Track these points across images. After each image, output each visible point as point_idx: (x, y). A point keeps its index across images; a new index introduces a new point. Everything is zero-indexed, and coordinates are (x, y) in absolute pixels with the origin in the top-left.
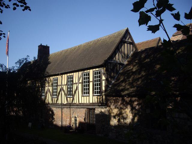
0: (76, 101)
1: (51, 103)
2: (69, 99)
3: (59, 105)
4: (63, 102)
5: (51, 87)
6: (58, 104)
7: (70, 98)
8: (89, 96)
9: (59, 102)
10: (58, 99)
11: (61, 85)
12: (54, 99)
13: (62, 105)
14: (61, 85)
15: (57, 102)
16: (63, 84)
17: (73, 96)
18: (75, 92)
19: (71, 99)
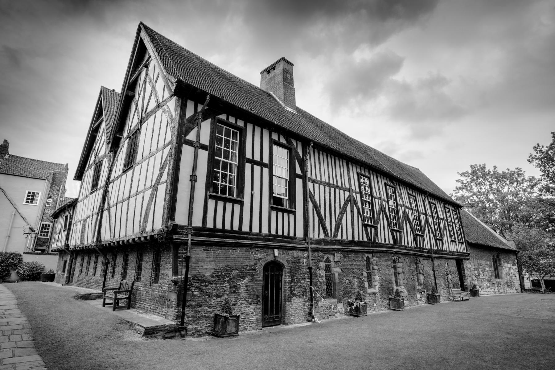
0: (446, 248)
2: (438, 241)
3: (428, 253)
9: (427, 246)
10: (424, 240)
11: (425, 214)
12: (418, 237)
13: (431, 251)
15: (423, 245)
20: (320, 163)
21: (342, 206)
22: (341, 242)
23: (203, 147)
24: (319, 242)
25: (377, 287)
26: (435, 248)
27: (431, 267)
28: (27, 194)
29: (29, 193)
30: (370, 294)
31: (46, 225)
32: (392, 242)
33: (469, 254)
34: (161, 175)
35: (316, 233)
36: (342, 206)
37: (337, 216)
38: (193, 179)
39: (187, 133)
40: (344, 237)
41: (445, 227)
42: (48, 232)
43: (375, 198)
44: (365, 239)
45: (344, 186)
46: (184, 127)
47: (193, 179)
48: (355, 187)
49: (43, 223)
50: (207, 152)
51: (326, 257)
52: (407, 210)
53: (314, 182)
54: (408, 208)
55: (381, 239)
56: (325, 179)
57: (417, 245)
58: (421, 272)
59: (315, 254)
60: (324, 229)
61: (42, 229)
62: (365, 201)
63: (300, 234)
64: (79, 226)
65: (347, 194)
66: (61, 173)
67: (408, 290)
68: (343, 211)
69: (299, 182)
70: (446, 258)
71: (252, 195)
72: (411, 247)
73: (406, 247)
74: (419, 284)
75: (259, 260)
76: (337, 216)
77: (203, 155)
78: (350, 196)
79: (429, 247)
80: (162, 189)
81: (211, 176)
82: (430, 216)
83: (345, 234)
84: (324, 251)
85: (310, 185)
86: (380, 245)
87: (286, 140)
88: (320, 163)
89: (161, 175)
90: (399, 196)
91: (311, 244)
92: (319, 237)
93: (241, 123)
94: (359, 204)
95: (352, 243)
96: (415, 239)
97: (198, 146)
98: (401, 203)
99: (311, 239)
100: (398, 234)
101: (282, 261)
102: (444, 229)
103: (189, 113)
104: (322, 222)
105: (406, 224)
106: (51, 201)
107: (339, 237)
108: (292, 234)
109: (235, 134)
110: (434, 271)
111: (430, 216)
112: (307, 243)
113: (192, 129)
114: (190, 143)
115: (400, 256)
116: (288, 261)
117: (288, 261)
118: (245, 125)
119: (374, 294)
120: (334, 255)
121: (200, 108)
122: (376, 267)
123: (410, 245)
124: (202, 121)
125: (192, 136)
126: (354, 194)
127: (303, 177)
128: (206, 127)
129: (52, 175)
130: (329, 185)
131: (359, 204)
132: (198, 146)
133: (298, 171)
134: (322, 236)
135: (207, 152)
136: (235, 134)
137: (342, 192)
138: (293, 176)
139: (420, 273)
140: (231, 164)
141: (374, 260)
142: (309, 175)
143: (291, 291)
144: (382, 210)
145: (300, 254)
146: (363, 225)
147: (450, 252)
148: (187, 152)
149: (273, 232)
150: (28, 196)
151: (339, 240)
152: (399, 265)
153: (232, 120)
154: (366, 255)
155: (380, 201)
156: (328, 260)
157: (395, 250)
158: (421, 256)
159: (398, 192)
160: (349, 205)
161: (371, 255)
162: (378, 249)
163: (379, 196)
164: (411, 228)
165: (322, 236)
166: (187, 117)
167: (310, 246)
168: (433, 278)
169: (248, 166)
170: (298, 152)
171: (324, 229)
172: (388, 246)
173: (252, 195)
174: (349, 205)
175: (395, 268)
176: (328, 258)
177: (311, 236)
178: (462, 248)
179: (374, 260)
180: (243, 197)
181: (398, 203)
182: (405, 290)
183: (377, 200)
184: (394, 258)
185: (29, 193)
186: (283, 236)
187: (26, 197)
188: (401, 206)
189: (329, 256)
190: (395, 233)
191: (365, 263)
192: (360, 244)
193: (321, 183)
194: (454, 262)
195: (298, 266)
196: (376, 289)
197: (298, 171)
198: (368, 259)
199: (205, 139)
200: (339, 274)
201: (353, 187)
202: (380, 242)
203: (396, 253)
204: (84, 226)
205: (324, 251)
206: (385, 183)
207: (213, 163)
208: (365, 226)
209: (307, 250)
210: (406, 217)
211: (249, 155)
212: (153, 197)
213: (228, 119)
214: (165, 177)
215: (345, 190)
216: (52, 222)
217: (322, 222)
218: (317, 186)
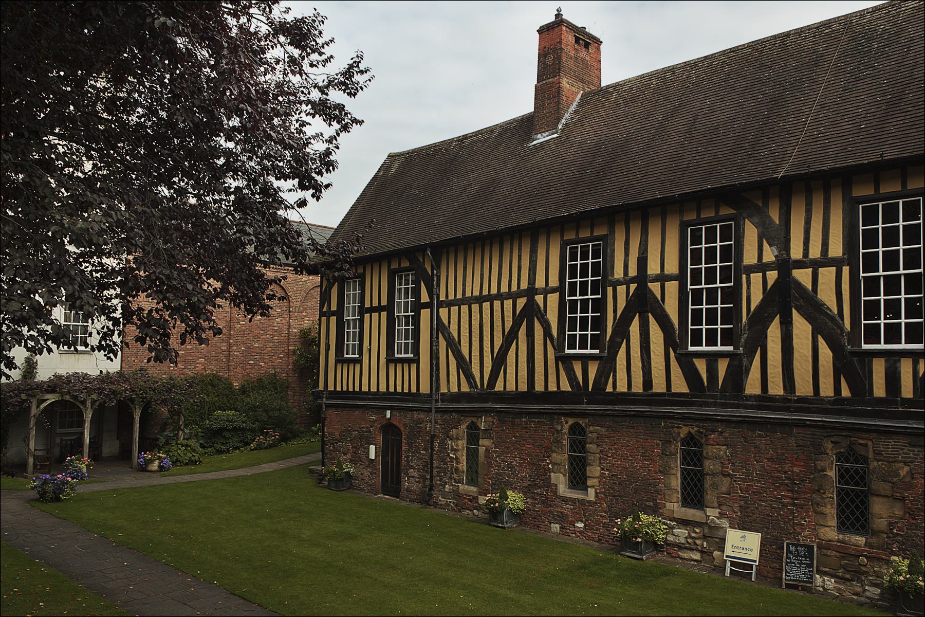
21: (507, 331)
22: (504, 397)
24: (459, 397)
25: (591, 491)
30: (566, 500)
35: (453, 383)
36: (507, 331)
37: (496, 351)
44: (566, 386)
58: (883, 487)
63: (425, 388)
65: (521, 302)
68: (510, 338)
69: (425, 314)
75: (375, 421)
76: (496, 351)
83: (513, 379)
84: (462, 412)
85: (443, 312)
92: (459, 389)
95: (530, 395)
101: (397, 424)
104: (464, 366)
105: (787, 324)
107: (499, 387)
108: (414, 390)
116: (405, 425)
117: (405, 425)
126: (539, 299)
130: (480, 300)
133: (425, 298)
134: (465, 388)
137: (508, 304)
141: (593, 432)
142: (442, 298)
143: (407, 461)
146: (557, 359)
149: (392, 390)
157: (694, 410)
162: (610, 407)
163: (633, 272)
165: (465, 388)
171: (469, 377)
172: (670, 398)
177: (444, 390)
179: (593, 432)
183: (622, 289)
186: (402, 393)
192: (547, 397)
193: (458, 303)
195: (418, 432)
196: (591, 495)
197: (425, 298)
200: (487, 450)
201: (540, 283)
205: (462, 412)
217: (464, 366)
218: (454, 309)
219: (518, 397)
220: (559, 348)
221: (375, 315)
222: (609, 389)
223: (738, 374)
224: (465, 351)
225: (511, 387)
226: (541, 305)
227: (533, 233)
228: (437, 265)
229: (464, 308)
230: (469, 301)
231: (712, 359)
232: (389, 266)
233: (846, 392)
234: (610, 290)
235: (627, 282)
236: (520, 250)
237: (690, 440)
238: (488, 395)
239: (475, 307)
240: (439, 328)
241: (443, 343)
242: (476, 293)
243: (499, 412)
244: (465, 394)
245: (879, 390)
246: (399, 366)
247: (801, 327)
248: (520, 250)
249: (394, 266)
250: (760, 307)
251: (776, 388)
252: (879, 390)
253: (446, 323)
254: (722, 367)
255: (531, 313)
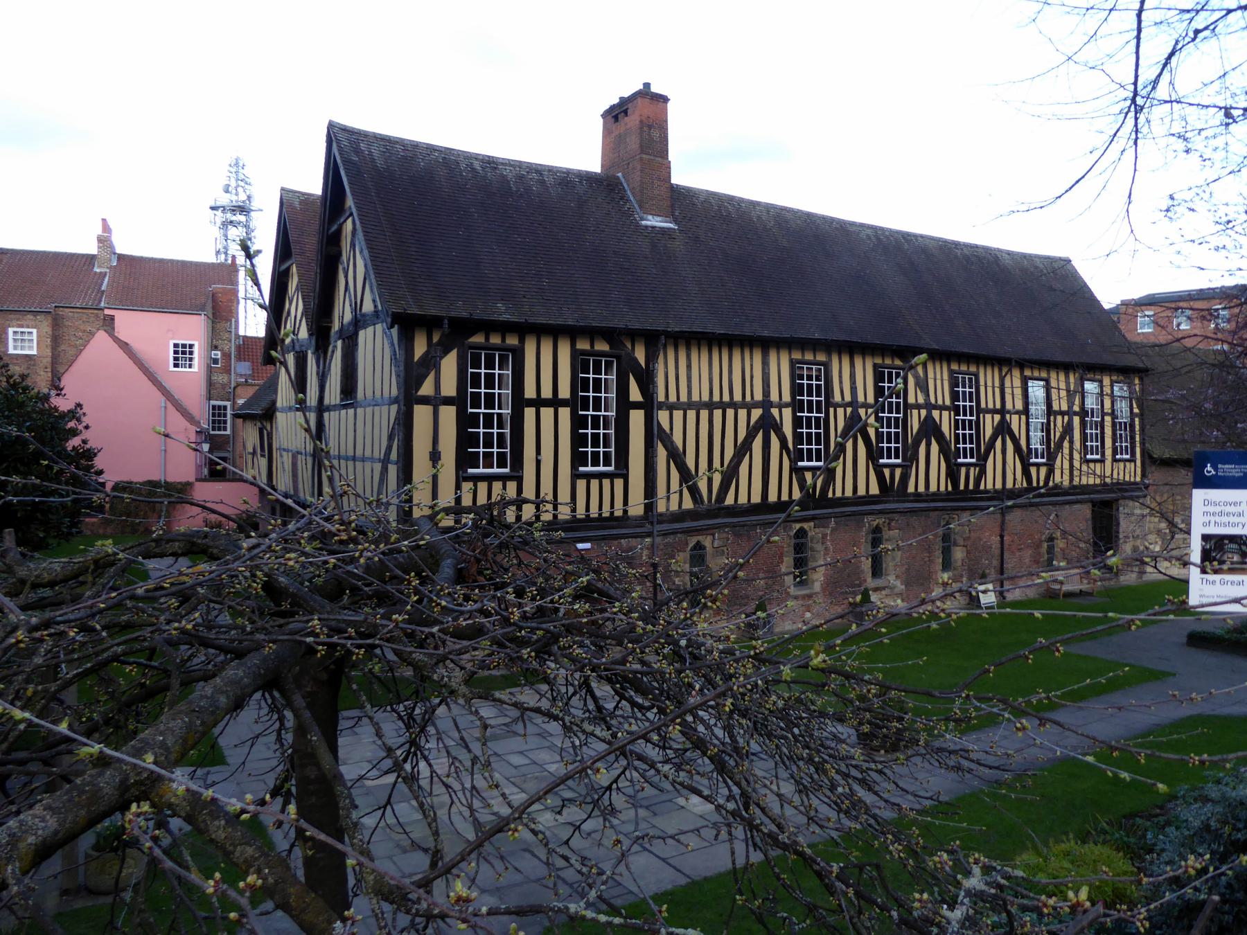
0: (1061, 478)
1: (942, 488)
2: (1033, 470)
4: (1009, 485)
5: (945, 414)
6: (986, 491)
7: (1038, 465)
8: (1102, 461)
9: (991, 482)
10: (983, 472)
11: (1002, 411)
12: (963, 470)
14: (854, 403)
16: (1009, 406)
17: (983, 459)
18: (1059, 446)
19: (1043, 470)
20: (689, 367)
22: (735, 511)
23: (448, 401)
24: (681, 516)
26: (1021, 483)
27: (997, 530)
28: (172, 349)
29: (176, 345)
31: (219, 407)
32: (875, 490)
33: (1147, 487)
34: (389, 448)
38: (435, 456)
39: (419, 385)
40: (743, 499)
41: (1068, 430)
42: (225, 422)
43: (836, 406)
45: (748, 398)
46: (412, 375)
47: (435, 456)
48: (781, 390)
49: (213, 402)
50: (454, 408)
51: (692, 541)
52: (936, 414)
53: (671, 408)
54: (942, 408)
55: (842, 488)
56: (701, 393)
57: (955, 484)
58: (961, 542)
59: (670, 539)
60: (694, 491)
61: (214, 415)
62: (809, 419)
63: (636, 509)
64: (287, 459)
65: (757, 413)
66: (225, 292)
67: (907, 584)
68: (743, 449)
69: (637, 419)
70: (1054, 504)
71: (538, 463)
72: (934, 494)
73: (919, 495)
74: (947, 566)
77: (448, 414)
78: (762, 417)
79: (999, 486)
80: (393, 470)
81: (465, 440)
82: (1017, 412)
84: (689, 532)
85: (663, 417)
86: (842, 502)
87: (609, 342)
88: (689, 367)
89: (389, 448)
90: (917, 384)
91: (659, 522)
93: (512, 341)
94: (788, 429)
95: (764, 507)
96: (952, 474)
97: (436, 401)
98: (921, 400)
99: (661, 515)
100: (898, 472)
102: (1062, 438)
103: (420, 348)
105: (928, 445)
106: (218, 354)
107: (730, 500)
109: (503, 360)
110: (1002, 537)
111: (1017, 412)
112: (652, 523)
113: (426, 377)
114: (425, 401)
115: (896, 516)
118: (522, 341)
119: (810, 596)
120: (713, 535)
121: (435, 339)
122: (819, 547)
123: (933, 488)
124: (441, 358)
125: (427, 389)
126: (775, 412)
127: (649, 405)
128: (449, 365)
129: (210, 301)
130: (710, 406)
131: (788, 429)
132: (436, 401)
133: (635, 395)
134: (688, 504)
135: (454, 408)
136: (503, 360)
137: (742, 413)
138: (625, 406)
139: (956, 544)
140: (499, 415)
142: (661, 398)
144: (854, 426)
145: (633, 542)
147: (1075, 487)
148: (422, 414)
150: (176, 352)
151: (728, 507)
152: (886, 534)
153: (495, 340)
154: (798, 526)
155: (849, 410)
156: (699, 546)
158: (964, 509)
159: (916, 377)
160: (760, 435)
161: (812, 524)
163: (848, 398)
164: (944, 450)
165: (688, 504)
166: (416, 359)
167: (658, 527)
168: (998, 552)
169: (529, 413)
170: (636, 360)
171: (694, 491)
172: (868, 499)
173: (538, 463)
174: (760, 435)
175: (876, 542)
176: (698, 542)
177: (661, 507)
178: (1130, 472)
180: (522, 469)
181: (911, 400)
182: (898, 583)
183: (840, 411)
184: (875, 523)
185: (176, 345)
186: (600, 518)
187: (171, 355)
188: (918, 407)
189: (700, 538)
190: (887, 472)
191: (793, 541)
193: (685, 407)
194: (1086, 511)
197: (635, 395)
198: (802, 533)
199: (449, 388)
201: (774, 397)
202: (839, 494)
203: (881, 512)
204: (294, 465)
206: (875, 366)
207: (465, 422)
208: (797, 471)
209: (649, 535)
210: (930, 429)
211: (530, 393)
212: (384, 470)
213: (487, 339)
214: (394, 456)
215: (749, 407)
216: (228, 400)
218: (678, 415)
219: (752, 509)
220: (793, 462)
221: (547, 413)
222: (830, 495)
223: (905, 478)
224: (690, 462)
225: (743, 499)
226: (778, 419)
227: (766, 344)
228: (651, 358)
229: (691, 414)
230: (698, 407)
231: (892, 467)
232: (573, 345)
233: (950, 488)
234: (832, 410)
235: (845, 406)
236: (751, 358)
237: (877, 530)
238: (719, 510)
239: (704, 414)
240: (653, 434)
241: (662, 453)
242: (706, 398)
243: (734, 526)
244: (689, 512)
245: (962, 487)
246: (595, 483)
247: (935, 447)
248: (751, 358)
249: (583, 345)
250: (918, 433)
251: (921, 489)
252: (962, 487)
253: (668, 430)
254: (898, 472)
255: (768, 425)
